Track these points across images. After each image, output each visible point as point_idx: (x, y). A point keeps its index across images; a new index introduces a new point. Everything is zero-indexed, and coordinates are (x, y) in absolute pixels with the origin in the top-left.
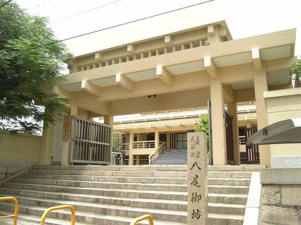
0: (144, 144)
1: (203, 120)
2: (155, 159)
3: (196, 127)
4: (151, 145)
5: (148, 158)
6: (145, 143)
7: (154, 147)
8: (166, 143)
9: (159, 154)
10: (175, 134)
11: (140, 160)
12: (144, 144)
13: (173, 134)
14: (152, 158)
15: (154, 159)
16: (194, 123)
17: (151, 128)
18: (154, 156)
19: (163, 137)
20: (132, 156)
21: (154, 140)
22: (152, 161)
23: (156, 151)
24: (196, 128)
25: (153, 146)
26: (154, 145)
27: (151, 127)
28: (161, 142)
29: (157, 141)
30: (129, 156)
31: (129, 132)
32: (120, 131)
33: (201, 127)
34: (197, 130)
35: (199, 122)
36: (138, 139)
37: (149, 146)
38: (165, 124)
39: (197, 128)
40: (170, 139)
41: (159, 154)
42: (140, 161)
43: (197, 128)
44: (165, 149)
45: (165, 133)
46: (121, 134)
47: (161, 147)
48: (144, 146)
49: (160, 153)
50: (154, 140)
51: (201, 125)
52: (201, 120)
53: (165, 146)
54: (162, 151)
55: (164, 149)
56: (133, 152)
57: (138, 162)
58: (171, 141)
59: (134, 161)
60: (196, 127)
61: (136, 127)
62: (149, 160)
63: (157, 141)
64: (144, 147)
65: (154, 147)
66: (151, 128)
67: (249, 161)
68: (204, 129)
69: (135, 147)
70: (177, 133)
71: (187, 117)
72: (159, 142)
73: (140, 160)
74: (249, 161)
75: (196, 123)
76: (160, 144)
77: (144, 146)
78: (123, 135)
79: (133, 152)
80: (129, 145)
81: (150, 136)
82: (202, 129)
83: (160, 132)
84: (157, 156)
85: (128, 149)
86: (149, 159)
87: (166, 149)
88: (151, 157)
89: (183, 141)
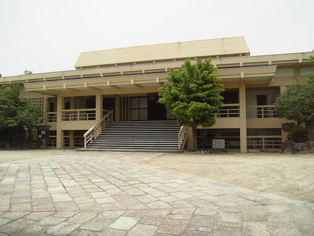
0: (78, 114)
1: (173, 77)
2: (95, 138)
3: (161, 88)
4: (89, 115)
5: (83, 138)
6: (81, 112)
7: (95, 119)
8: (114, 112)
9: (103, 129)
10: (128, 98)
11: (76, 137)
12: (78, 114)
13: (124, 98)
14: (90, 137)
15: (93, 138)
16: (157, 81)
17: (88, 89)
18: (93, 135)
19: (109, 102)
20: (60, 132)
21: (95, 108)
22: (90, 141)
23: (98, 124)
24: (161, 90)
25: (92, 117)
26: (95, 115)
27: (111, 86)
28: (105, 110)
29: (98, 109)
30: (56, 131)
31: (56, 95)
32: (43, 93)
33: (170, 87)
34: (163, 93)
35: (167, 81)
36: (72, 105)
37: (88, 117)
38: (134, 81)
39: (163, 89)
40: (121, 107)
41: (103, 129)
42: (75, 139)
43: (163, 89)
44: (112, 120)
45: (114, 97)
46: (46, 97)
47: (106, 119)
48: (78, 117)
49: (104, 128)
50: (95, 108)
51: (171, 84)
52: (170, 77)
53: (112, 117)
54: (108, 126)
55: (111, 121)
56: (62, 126)
57: (72, 142)
58: (121, 112)
59: (65, 138)
60: (161, 88)
61: (64, 87)
62: (85, 141)
63: (98, 109)
64: (78, 119)
65: (95, 119)
66: (88, 89)
67: (50, 136)
68: (175, 91)
69: (66, 118)
70: (131, 98)
71: (29, 81)
72: (102, 110)
73: (76, 137)
74: (50, 136)
75: (161, 81)
76: (104, 113)
77: (78, 117)
78: (49, 99)
79: (62, 126)
80: (56, 115)
81: (90, 102)
82: (172, 92)
83: (103, 96)
84: (98, 133)
85: (55, 121)
86: (85, 139)
87: (114, 120)
88: (87, 136)
89: (139, 109)
